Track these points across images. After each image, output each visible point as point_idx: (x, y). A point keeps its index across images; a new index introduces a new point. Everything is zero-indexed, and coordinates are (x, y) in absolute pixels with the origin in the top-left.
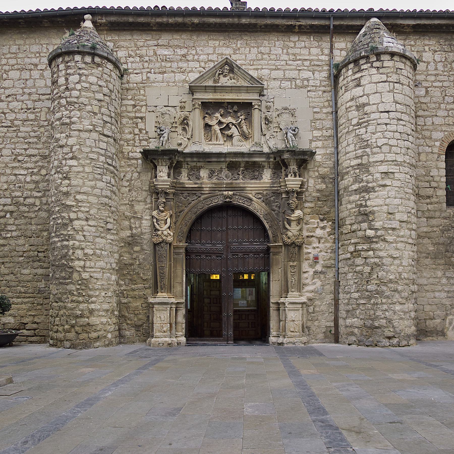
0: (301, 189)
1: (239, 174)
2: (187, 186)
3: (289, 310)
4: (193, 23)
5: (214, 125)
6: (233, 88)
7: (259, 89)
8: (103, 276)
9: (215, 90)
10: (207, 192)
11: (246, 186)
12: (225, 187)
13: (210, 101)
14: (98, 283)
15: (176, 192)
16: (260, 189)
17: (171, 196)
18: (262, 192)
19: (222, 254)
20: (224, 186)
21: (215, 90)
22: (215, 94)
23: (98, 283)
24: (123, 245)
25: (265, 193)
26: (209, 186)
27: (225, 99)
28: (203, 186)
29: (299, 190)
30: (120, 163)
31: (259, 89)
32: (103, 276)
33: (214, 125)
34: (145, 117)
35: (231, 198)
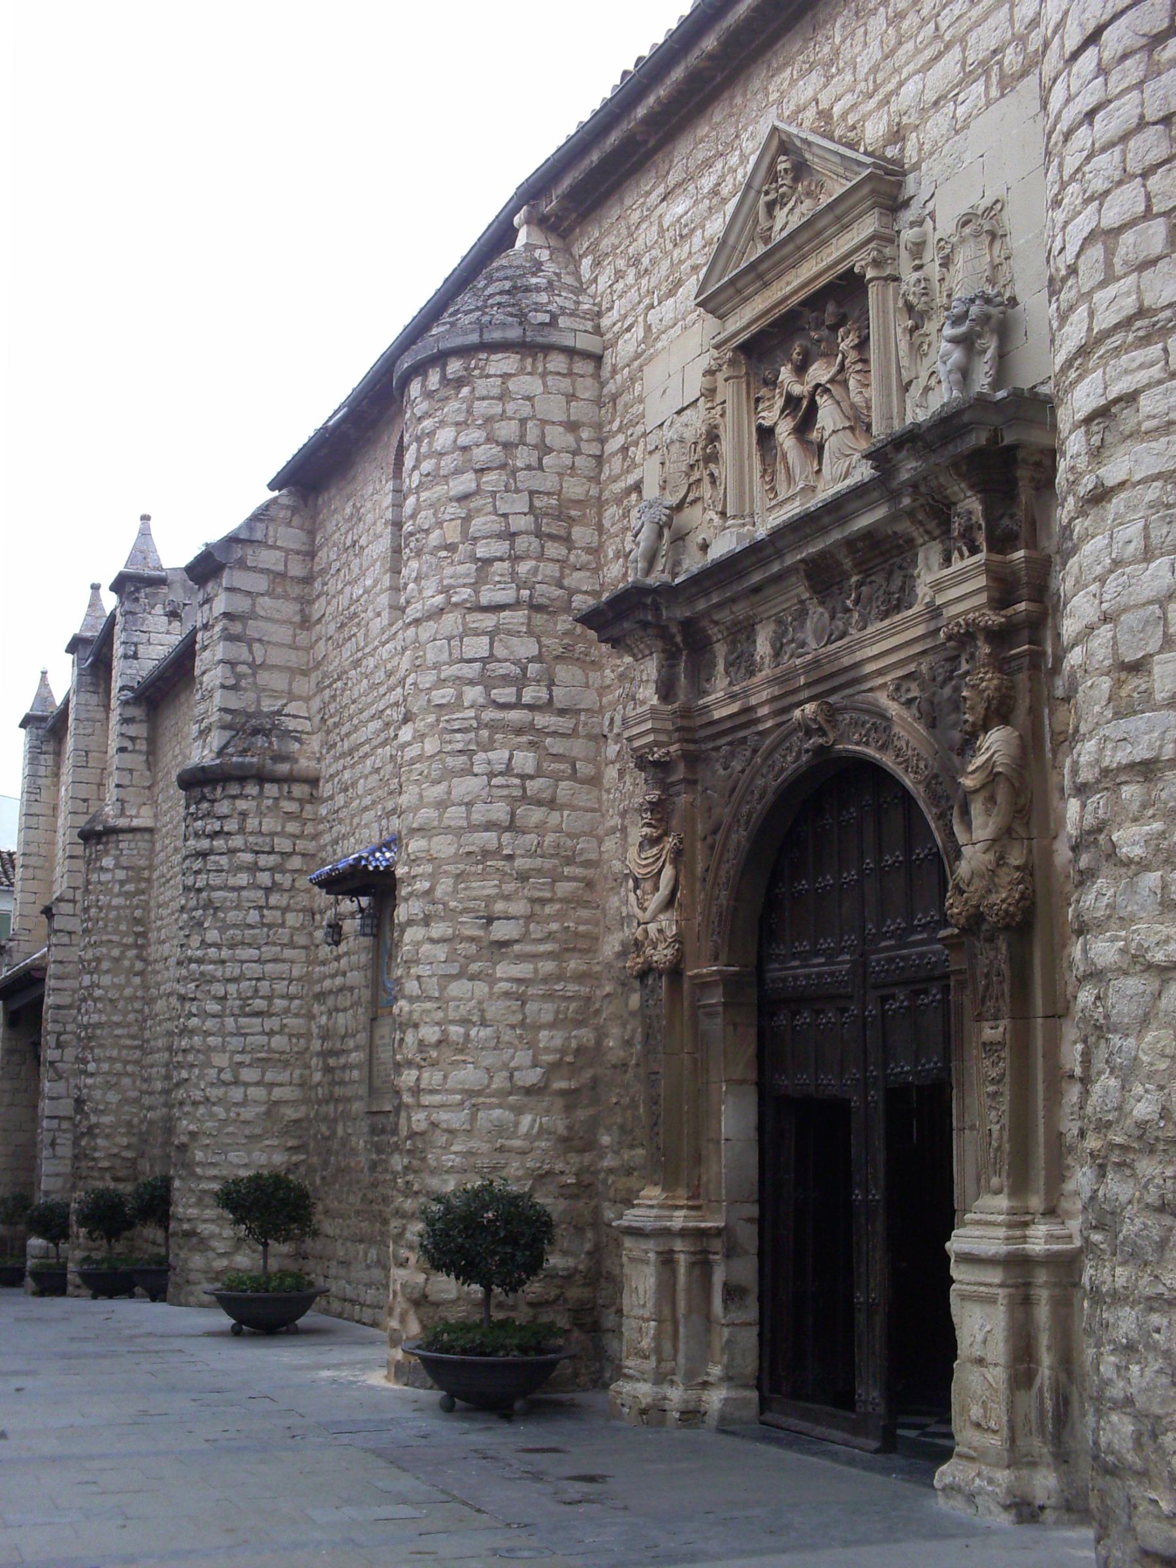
0: (1010, 611)
1: (847, 610)
2: (717, 715)
3: (964, 1297)
4: (711, 57)
5: (776, 424)
6: (799, 241)
7: (866, 190)
8: (473, 1118)
9: (760, 277)
10: (769, 724)
11: (859, 656)
12: (808, 685)
13: (754, 328)
14: (454, 1148)
15: (692, 747)
16: (902, 655)
17: (680, 773)
18: (912, 667)
19: (850, 997)
20: (802, 681)
21: (760, 277)
22: (767, 293)
23: (454, 1148)
24: (608, 989)
25: (924, 668)
26: (765, 695)
27: (786, 298)
28: (753, 701)
29: (994, 619)
30: (603, 677)
31: (866, 190)
32: (473, 1118)
33: (776, 424)
34: (641, 481)
35: (821, 731)
